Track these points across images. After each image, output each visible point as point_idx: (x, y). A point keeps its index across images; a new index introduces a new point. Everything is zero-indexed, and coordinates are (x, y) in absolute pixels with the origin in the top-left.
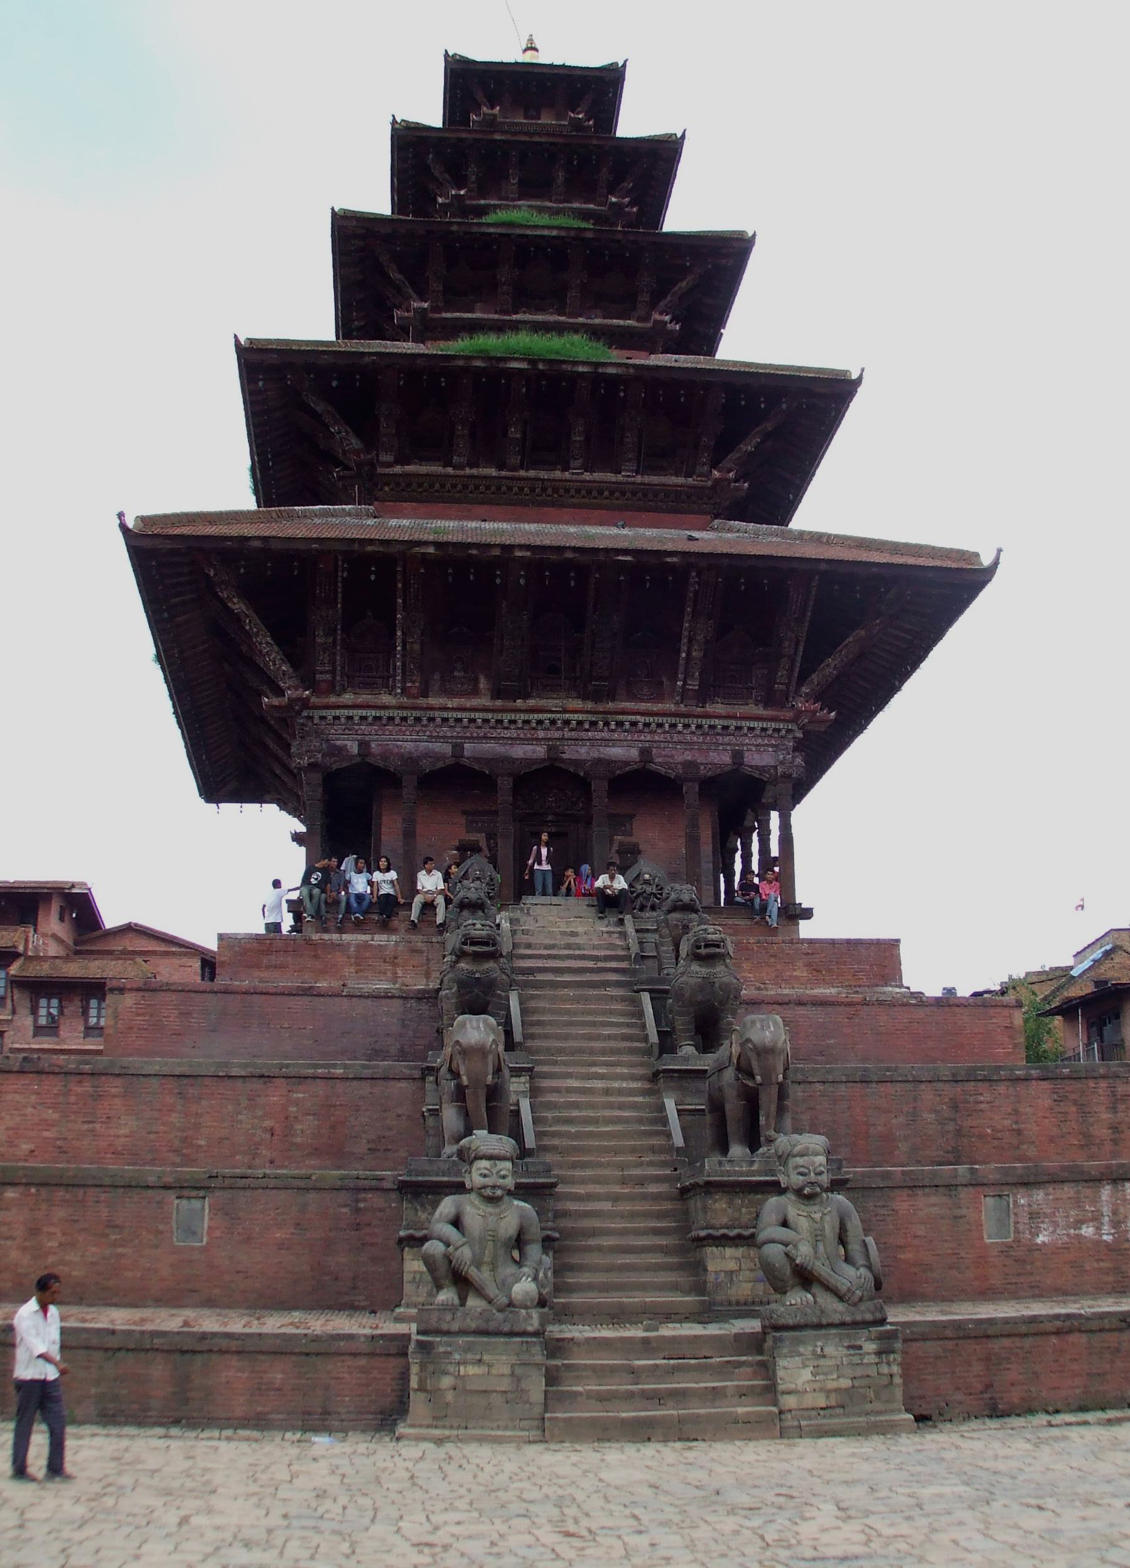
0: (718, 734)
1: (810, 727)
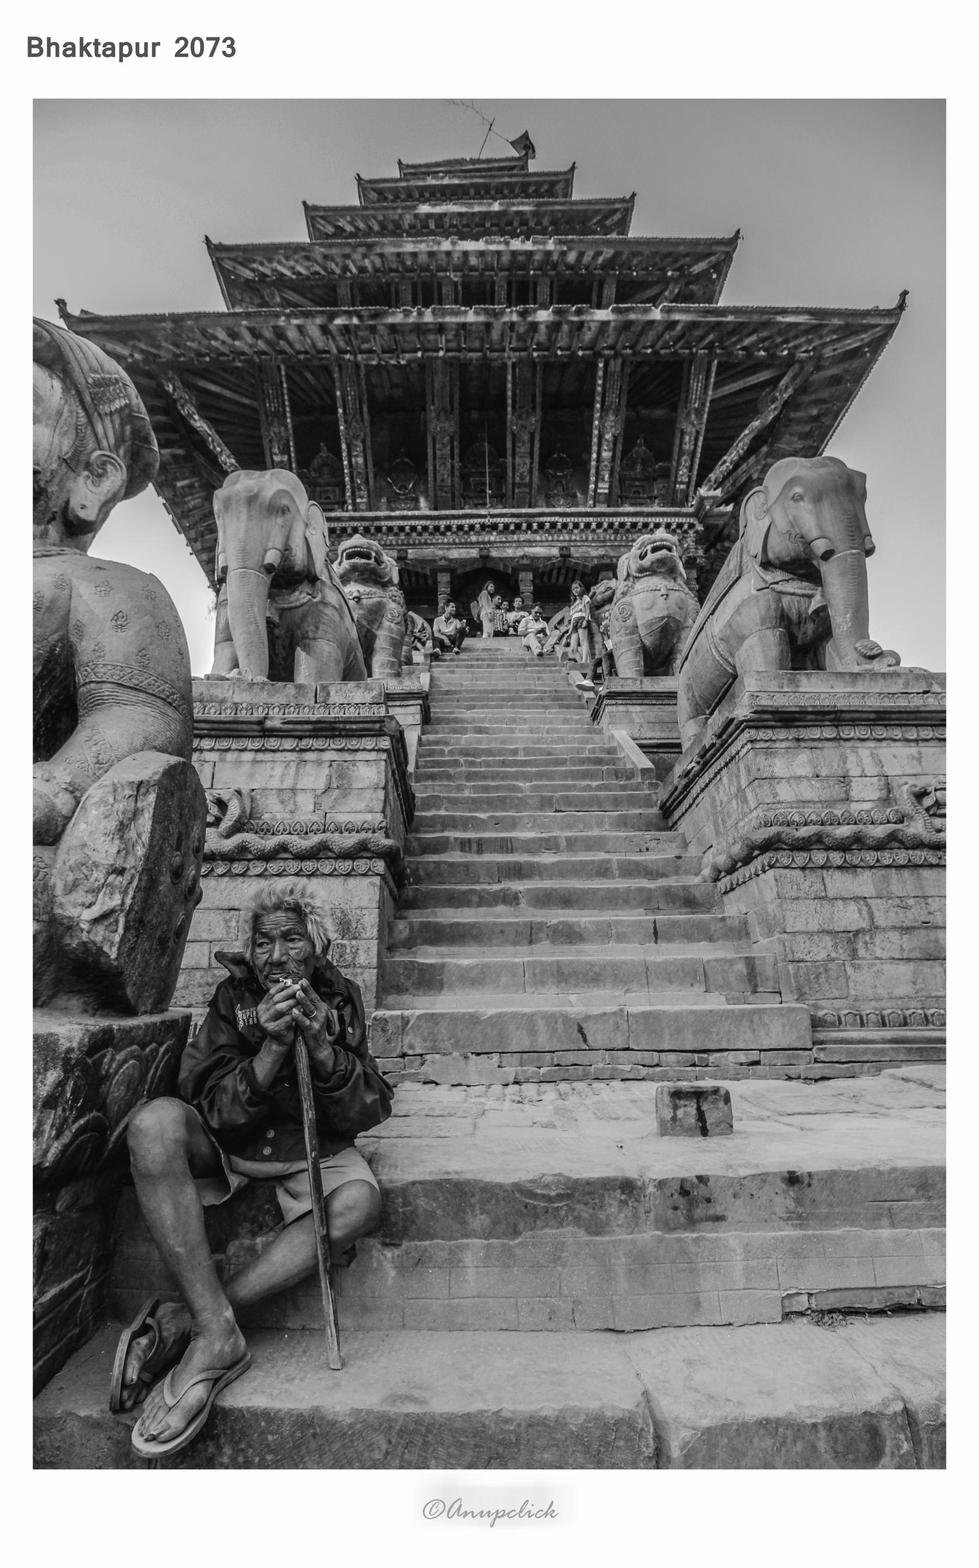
0: (628, 531)
1: (710, 521)
